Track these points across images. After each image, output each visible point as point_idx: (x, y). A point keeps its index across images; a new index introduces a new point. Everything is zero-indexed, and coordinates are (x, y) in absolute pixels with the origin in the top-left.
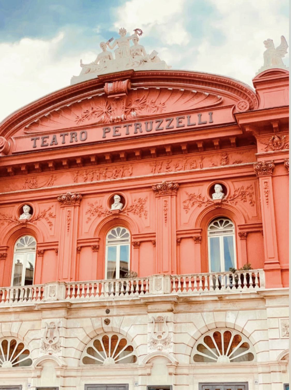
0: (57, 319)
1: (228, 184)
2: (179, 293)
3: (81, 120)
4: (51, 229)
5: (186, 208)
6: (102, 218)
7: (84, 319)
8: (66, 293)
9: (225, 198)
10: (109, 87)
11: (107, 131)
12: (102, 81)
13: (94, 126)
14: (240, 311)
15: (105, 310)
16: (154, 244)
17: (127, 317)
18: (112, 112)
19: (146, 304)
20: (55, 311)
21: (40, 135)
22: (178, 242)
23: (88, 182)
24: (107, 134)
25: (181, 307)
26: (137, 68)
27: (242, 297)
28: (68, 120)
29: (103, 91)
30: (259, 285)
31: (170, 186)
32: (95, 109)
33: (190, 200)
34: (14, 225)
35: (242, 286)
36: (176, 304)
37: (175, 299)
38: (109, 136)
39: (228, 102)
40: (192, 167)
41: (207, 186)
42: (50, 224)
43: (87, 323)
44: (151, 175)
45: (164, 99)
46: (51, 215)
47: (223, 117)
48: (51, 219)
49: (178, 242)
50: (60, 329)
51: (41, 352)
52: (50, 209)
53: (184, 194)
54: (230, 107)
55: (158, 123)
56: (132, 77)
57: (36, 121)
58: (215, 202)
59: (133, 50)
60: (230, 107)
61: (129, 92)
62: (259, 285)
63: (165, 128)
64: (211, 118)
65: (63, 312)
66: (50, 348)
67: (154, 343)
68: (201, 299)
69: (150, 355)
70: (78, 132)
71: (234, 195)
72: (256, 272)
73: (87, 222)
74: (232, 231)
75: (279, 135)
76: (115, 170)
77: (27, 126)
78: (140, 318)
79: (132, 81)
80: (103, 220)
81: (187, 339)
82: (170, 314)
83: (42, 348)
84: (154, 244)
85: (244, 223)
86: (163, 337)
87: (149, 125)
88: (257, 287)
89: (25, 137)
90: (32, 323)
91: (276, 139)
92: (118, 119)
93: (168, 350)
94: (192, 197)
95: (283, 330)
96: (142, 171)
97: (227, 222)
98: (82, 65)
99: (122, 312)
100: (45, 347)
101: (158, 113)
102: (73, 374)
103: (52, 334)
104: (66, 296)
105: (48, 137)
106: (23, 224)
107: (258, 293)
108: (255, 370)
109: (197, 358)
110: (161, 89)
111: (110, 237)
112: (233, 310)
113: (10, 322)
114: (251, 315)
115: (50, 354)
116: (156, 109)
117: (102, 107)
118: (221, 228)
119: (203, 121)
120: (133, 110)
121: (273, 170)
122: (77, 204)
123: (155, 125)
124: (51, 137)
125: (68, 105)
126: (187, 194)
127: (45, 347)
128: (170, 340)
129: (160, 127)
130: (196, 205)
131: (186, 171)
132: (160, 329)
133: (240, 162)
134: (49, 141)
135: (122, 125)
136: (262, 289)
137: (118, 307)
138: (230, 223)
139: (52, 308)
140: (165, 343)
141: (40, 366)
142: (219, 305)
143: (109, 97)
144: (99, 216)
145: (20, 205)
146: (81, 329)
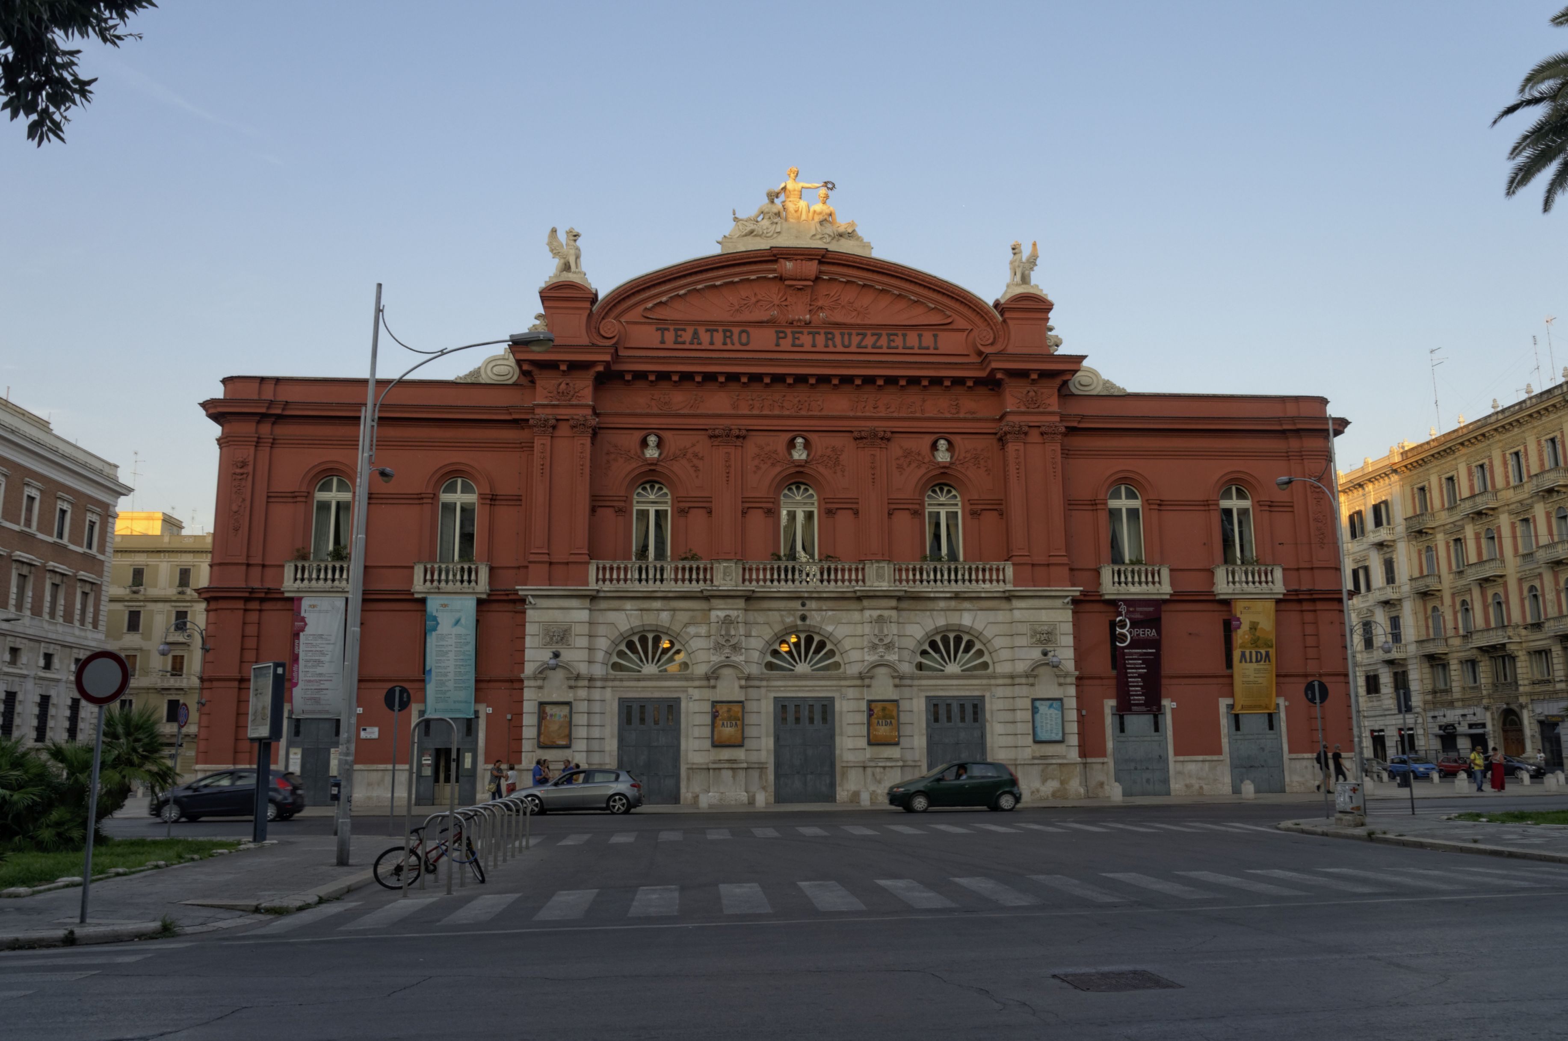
0: (735, 610)
1: (957, 439)
2: (904, 587)
3: (737, 310)
4: (697, 477)
5: (900, 467)
6: (778, 469)
7: (770, 613)
9: (953, 460)
11: (782, 335)
12: (776, 255)
13: (759, 324)
14: (979, 612)
15: (800, 602)
16: (856, 513)
17: (830, 613)
18: (789, 308)
19: (859, 599)
20: (730, 601)
21: (670, 324)
22: (890, 514)
23: (756, 412)
24: (782, 342)
25: (904, 604)
27: (983, 595)
28: (718, 307)
29: (775, 271)
30: (1004, 581)
31: (881, 434)
32: (760, 297)
33: (906, 457)
34: (634, 465)
36: (899, 599)
37: (902, 594)
38: (786, 344)
39: (961, 323)
40: (910, 410)
41: (928, 440)
42: (696, 469)
43: (775, 616)
44: (851, 414)
45: (866, 300)
46: (696, 455)
48: (696, 461)
49: (890, 514)
50: (740, 625)
51: (713, 654)
52: (694, 445)
53: (896, 448)
54: (963, 330)
55: (860, 337)
56: (823, 257)
57: (664, 299)
58: (941, 465)
59: (820, 213)
60: (963, 330)
61: (817, 279)
62: (1004, 581)
63: (870, 346)
64: (936, 342)
65: (741, 603)
66: (727, 651)
67: (874, 647)
68: (932, 595)
69: (872, 663)
70: (736, 331)
71: (965, 458)
72: (1001, 564)
73: (755, 472)
74: (957, 505)
75: (1035, 389)
76: (798, 399)
79: (821, 262)
80: (780, 473)
81: (911, 644)
82: (894, 613)
83: (715, 649)
84: (856, 513)
85: (976, 497)
86: (886, 641)
87: (846, 337)
88: (1001, 583)
89: (644, 323)
90: (690, 613)
91: (1032, 394)
92: (799, 320)
93: (892, 657)
94: (907, 454)
95: (1032, 637)
96: (838, 404)
97: (949, 492)
98: (736, 219)
99: (825, 605)
100: (718, 647)
101: (859, 322)
102: (757, 683)
103: (728, 631)
104: (744, 580)
105: (684, 330)
106: (652, 464)
107: (1004, 592)
108: (993, 682)
109: (920, 666)
110: (864, 286)
111: (785, 496)
112: (970, 610)
113: (657, 610)
114: (991, 616)
115: (727, 657)
116: (855, 313)
117: (773, 293)
118: (942, 499)
119: (924, 344)
120: (821, 308)
121: (1026, 434)
122: (738, 444)
123: (856, 340)
126: (901, 447)
127: (718, 647)
128: (894, 645)
129: (863, 344)
131: (901, 415)
132: (881, 631)
133: (974, 413)
135: (805, 331)
136: (1009, 587)
138: (954, 492)
140: (889, 647)
142: (953, 604)
143: (787, 283)
144: (773, 465)
145: (645, 432)
146: (767, 626)
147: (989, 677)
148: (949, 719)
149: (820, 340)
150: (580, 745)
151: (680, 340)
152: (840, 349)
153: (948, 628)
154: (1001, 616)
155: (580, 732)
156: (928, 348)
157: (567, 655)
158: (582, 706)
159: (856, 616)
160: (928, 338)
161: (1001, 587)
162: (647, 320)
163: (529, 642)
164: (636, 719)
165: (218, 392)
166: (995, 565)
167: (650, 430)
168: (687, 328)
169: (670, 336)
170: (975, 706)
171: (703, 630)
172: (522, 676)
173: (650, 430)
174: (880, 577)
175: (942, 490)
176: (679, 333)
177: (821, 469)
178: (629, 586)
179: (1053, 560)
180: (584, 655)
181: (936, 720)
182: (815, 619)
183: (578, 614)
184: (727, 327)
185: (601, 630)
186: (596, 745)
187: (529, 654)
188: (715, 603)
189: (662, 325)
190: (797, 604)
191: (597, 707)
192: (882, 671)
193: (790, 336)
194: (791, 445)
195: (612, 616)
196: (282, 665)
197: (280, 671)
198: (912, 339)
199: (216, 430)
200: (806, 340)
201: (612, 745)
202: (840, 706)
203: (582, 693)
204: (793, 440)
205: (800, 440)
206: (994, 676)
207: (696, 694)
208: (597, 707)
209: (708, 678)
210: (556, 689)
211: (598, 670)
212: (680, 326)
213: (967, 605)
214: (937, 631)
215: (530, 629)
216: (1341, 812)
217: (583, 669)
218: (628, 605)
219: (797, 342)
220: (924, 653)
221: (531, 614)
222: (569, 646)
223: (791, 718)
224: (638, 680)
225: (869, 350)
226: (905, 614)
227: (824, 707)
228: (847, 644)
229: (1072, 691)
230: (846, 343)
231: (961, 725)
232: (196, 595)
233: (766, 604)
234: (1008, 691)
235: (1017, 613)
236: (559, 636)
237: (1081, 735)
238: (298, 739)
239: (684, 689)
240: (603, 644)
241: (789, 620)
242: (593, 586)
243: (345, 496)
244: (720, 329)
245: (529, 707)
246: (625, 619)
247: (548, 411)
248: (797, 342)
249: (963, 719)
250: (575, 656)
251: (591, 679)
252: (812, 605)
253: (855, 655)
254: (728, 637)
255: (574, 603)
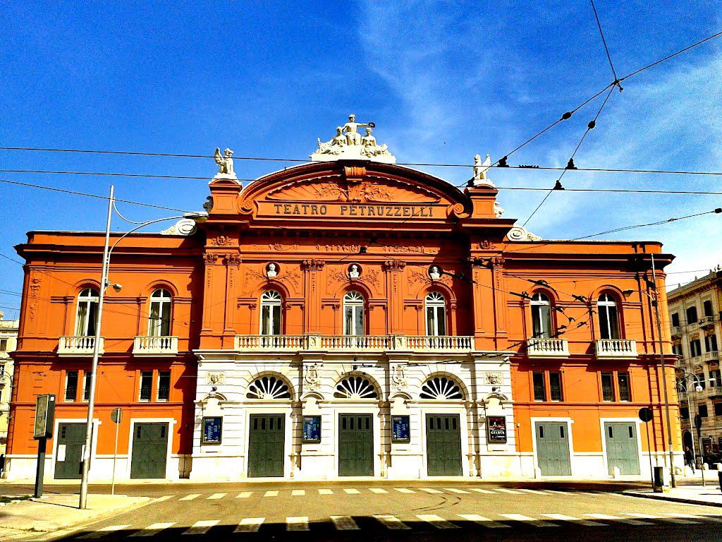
5: (410, 281)
6: (342, 283)
8: (322, 343)
10: (348, 170)
26: (373, 159)
28: (308, 193)
30: (470, 347)
35: (459, 347)
38: (347, 214)
45: (393, 189)
47: (439, 213)
57: (279, 188)
77: (271, 192)
92: (354, 200)
94: (415, 274)
104: (322, 346)
124: (293, 205)
125: (309, 180)
130: (418, 281)
134: (292, 209)
135: (358, 206)
148: (439, 428)
149: (366, 211)
151: (287, 211)
152: (377, 216)
156: (427, 216)
160: (426, 210)
162: (268, 200)
163: (199, 381)
164: (260, 427)
165: (25, 241)
166: (464, 337)
167: (272, 262)
168: (292, 204)
169: (282, 209)
170: (454, 420)
172: (195, 401)
173: (272, 262)
175: (435, 295)
176: (287, 207)
177: (366, 283)
179: (498, 335)
181: (432, 427)
184: (315, 203)
187: (199, 389)
189: (278, 203)
193: (349, 209)
194: (350, 269)
196: (54, 396)
197: (52, 399)
198: (417, 209)
199: (24, 261)
200: (358, 211)
204: (351, 266)
205: (355, 267)
210: (212, 409)
212: (288, 203)
214: (431, 375)
219: (353, 212)
223: (348, 425)
224: (261, 403)
225: (393, 217)
227: (367, 419)
229: (511, 411)
230: (380, 212)
231: (447, 431)
232: (9, 356)
237: (517, 437)
238: (64, 440)
242: (237, 348)
243: (95, 299)
244: (310, 205)
247: (214, 251)
248: (353, 212)
249: (447, 428)
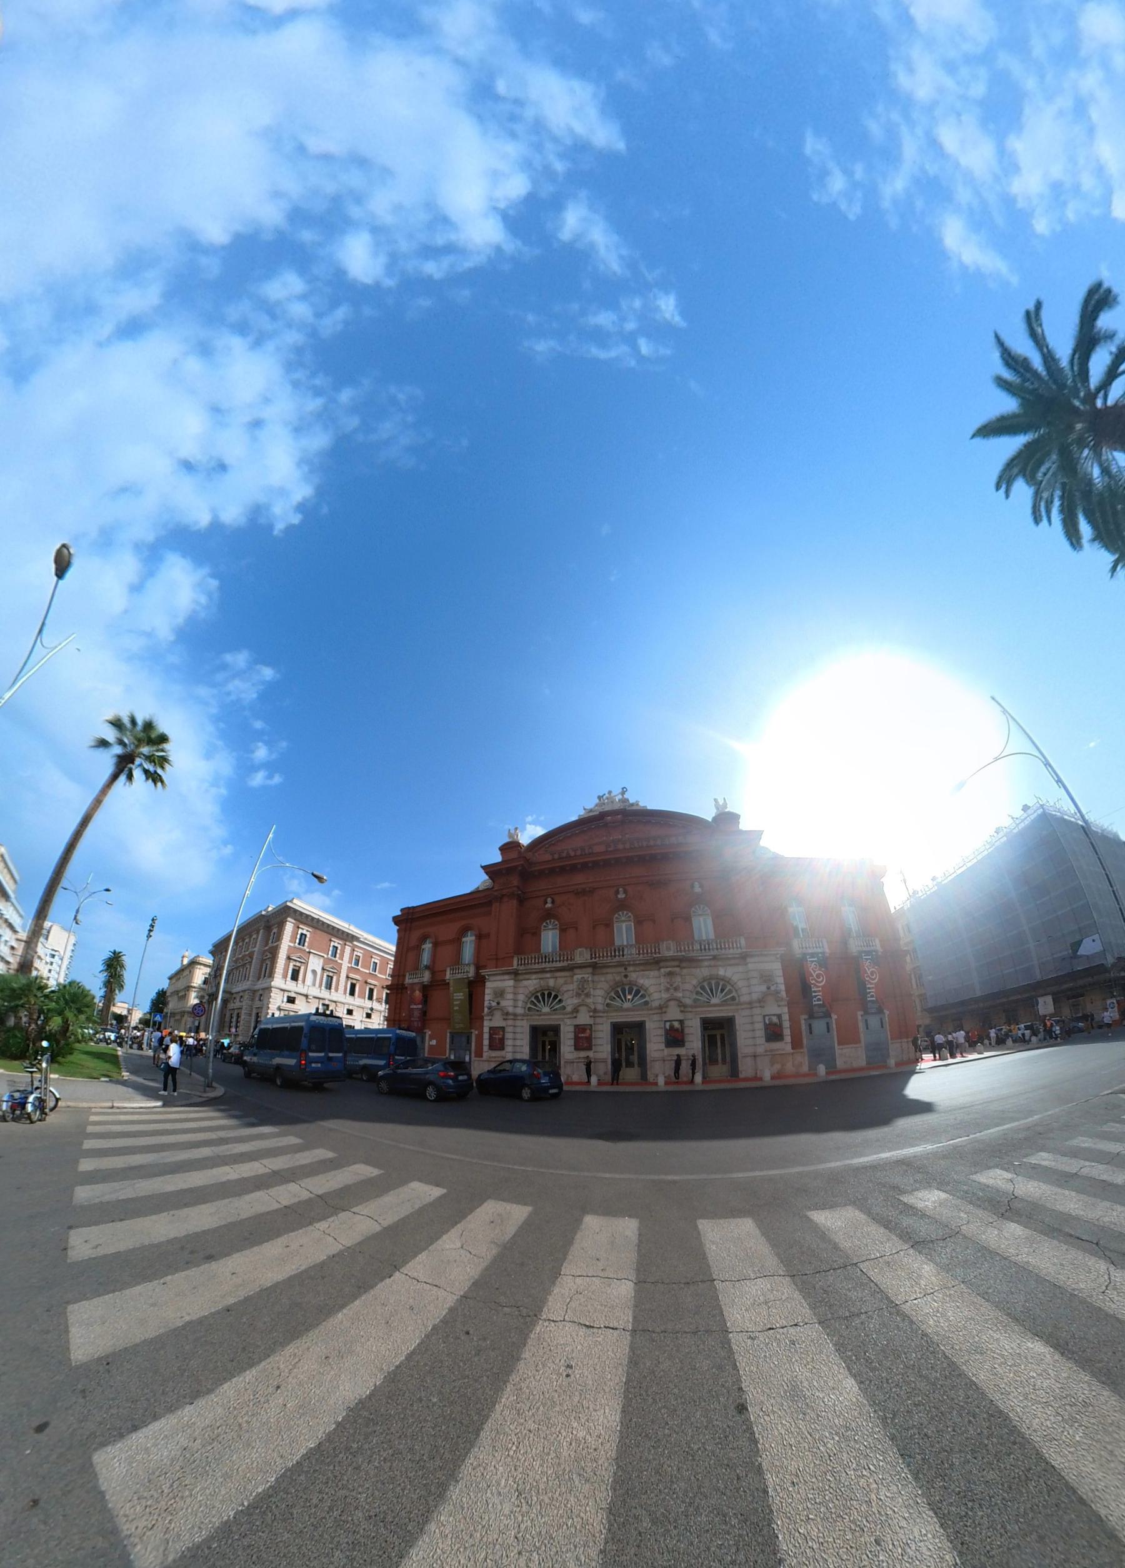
0: (586, 974)
25: (684, 965)
43: (609, 977)
65: (590, 970)
78: (652, 973)
82: (677, 969)
127: (578, 995)
137: (634, 965)
139: (582, 967)
141: (576, 1010)
142: (713, 963)
147: (737, 1005)
150: (509, 1049)
153: (711, 978)
154: (740, 969)
155: (508, 1042)
157: (503, 1003)
158: (508, 1029)
159: (656, 973)
161: (739, 951)
171: (571, 987)
174: (668, 949)
178: (534, 967)
180: (511, 1003)
182: (633, 976)
183: (508, 983)
185: (521, 990)
186: (518, 1049)
188: (577, 971)
190: (622, 969)
191: (518, 1030)
192: (672, 1003)
195: (526, 983)
201: (526, 1049)
202: (648, 1025)
203: (510, 1022)
206: (739, 1004)
207: (568, 1022)
208: (518, 1030)
209: (572, 1012)
210: (498, 1021)
211: (520, 1011)
213: (720, 963)
215: (487, 991)
216: (589, 1074)
217: (511, 1010)
218: (534, 976)
220: (697, 993)
221: (488, 984)
222: (503, 998)
226: (685, 971)
228: (652, 990)
233: (605, 971)
234: (747, 1012)
235: (750, 966)
236: (500, 994)
239: (563, 1020)
240: (521, 997)
241: (618, 978)
245: (486, 1030)
246: (532, 984)
250: (507, 1003)
251: (515, 1015)
252: (631, 969)
253: (656, 996)
254: (583, 989)
255: (506, 977)
